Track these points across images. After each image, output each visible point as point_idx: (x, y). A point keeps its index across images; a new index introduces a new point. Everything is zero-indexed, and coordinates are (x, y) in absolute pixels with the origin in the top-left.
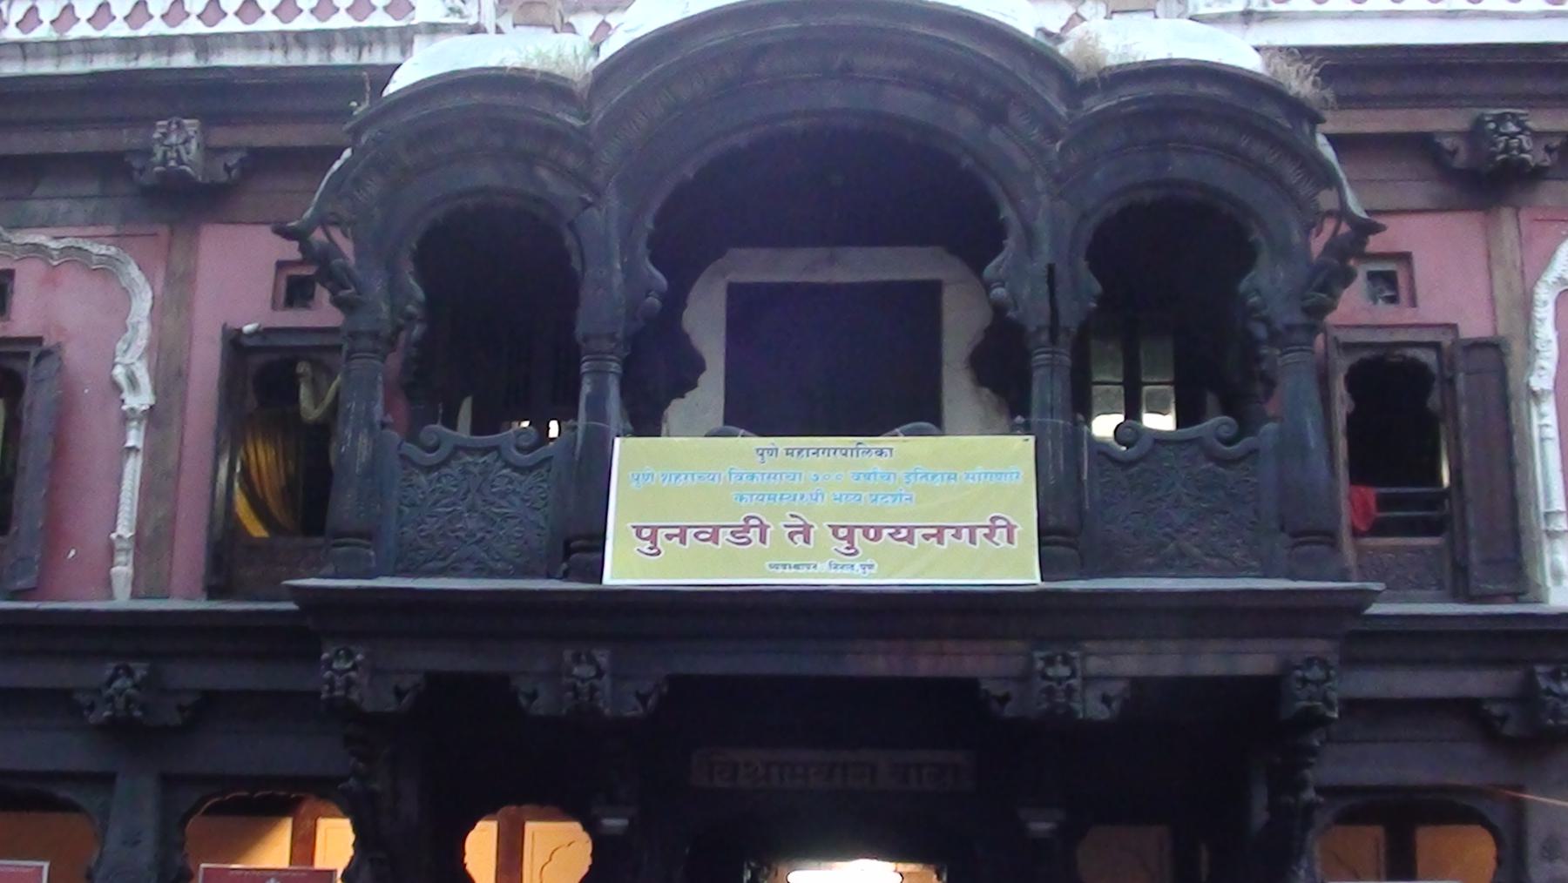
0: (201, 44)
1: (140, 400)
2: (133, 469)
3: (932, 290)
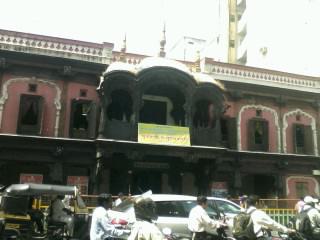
0: (69, 54)
1: (59, 108)
2: (58, 119)
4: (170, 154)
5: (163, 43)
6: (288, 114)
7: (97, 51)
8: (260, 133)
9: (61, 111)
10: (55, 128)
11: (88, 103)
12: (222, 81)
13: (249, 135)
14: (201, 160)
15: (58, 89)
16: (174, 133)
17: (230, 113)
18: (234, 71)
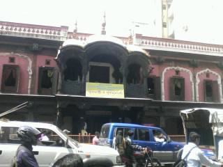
0: (37, 35)
1: (31, 73)
2: (30, 81)
3: (109, 68)
4: (110, 104)
5: (104, 25)
6: (200, 73)
7: (57, 32)
8: (178, 88)
9: (32, 75)
10: (29, 88)
11: (52, 69)
12: (147, 50)
13: (170, 88)
14: (133, 108)
15: (29, 60)
16: (104, 89)
17: (155, 73)
18: (158, 42)
